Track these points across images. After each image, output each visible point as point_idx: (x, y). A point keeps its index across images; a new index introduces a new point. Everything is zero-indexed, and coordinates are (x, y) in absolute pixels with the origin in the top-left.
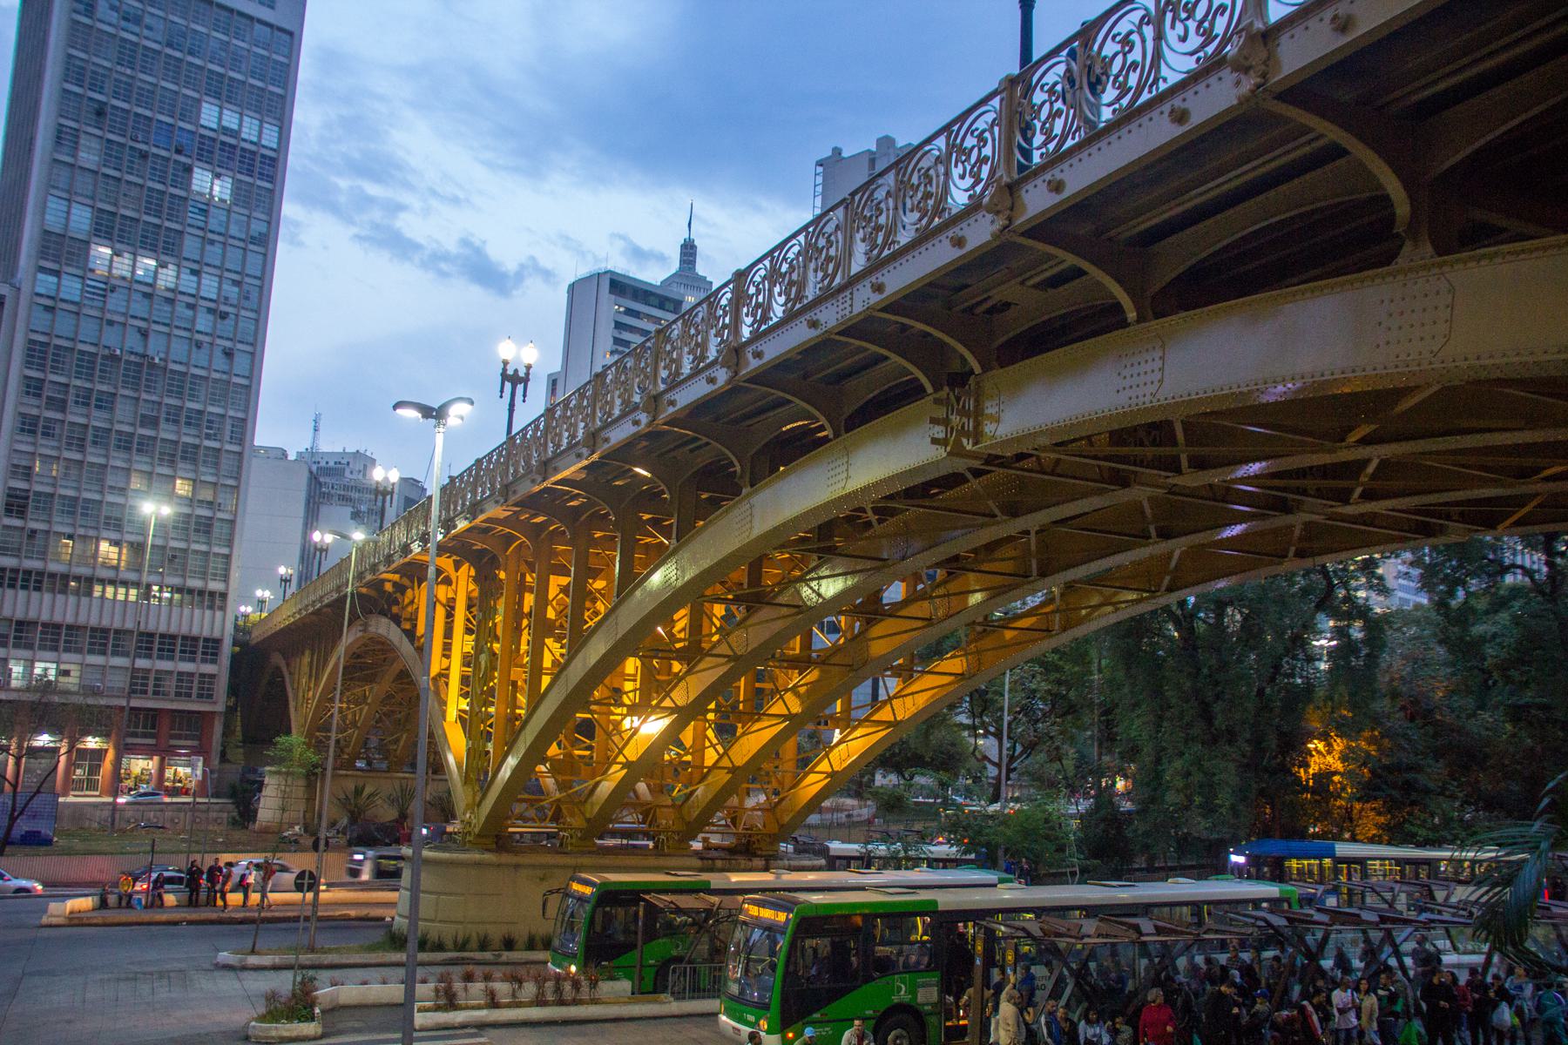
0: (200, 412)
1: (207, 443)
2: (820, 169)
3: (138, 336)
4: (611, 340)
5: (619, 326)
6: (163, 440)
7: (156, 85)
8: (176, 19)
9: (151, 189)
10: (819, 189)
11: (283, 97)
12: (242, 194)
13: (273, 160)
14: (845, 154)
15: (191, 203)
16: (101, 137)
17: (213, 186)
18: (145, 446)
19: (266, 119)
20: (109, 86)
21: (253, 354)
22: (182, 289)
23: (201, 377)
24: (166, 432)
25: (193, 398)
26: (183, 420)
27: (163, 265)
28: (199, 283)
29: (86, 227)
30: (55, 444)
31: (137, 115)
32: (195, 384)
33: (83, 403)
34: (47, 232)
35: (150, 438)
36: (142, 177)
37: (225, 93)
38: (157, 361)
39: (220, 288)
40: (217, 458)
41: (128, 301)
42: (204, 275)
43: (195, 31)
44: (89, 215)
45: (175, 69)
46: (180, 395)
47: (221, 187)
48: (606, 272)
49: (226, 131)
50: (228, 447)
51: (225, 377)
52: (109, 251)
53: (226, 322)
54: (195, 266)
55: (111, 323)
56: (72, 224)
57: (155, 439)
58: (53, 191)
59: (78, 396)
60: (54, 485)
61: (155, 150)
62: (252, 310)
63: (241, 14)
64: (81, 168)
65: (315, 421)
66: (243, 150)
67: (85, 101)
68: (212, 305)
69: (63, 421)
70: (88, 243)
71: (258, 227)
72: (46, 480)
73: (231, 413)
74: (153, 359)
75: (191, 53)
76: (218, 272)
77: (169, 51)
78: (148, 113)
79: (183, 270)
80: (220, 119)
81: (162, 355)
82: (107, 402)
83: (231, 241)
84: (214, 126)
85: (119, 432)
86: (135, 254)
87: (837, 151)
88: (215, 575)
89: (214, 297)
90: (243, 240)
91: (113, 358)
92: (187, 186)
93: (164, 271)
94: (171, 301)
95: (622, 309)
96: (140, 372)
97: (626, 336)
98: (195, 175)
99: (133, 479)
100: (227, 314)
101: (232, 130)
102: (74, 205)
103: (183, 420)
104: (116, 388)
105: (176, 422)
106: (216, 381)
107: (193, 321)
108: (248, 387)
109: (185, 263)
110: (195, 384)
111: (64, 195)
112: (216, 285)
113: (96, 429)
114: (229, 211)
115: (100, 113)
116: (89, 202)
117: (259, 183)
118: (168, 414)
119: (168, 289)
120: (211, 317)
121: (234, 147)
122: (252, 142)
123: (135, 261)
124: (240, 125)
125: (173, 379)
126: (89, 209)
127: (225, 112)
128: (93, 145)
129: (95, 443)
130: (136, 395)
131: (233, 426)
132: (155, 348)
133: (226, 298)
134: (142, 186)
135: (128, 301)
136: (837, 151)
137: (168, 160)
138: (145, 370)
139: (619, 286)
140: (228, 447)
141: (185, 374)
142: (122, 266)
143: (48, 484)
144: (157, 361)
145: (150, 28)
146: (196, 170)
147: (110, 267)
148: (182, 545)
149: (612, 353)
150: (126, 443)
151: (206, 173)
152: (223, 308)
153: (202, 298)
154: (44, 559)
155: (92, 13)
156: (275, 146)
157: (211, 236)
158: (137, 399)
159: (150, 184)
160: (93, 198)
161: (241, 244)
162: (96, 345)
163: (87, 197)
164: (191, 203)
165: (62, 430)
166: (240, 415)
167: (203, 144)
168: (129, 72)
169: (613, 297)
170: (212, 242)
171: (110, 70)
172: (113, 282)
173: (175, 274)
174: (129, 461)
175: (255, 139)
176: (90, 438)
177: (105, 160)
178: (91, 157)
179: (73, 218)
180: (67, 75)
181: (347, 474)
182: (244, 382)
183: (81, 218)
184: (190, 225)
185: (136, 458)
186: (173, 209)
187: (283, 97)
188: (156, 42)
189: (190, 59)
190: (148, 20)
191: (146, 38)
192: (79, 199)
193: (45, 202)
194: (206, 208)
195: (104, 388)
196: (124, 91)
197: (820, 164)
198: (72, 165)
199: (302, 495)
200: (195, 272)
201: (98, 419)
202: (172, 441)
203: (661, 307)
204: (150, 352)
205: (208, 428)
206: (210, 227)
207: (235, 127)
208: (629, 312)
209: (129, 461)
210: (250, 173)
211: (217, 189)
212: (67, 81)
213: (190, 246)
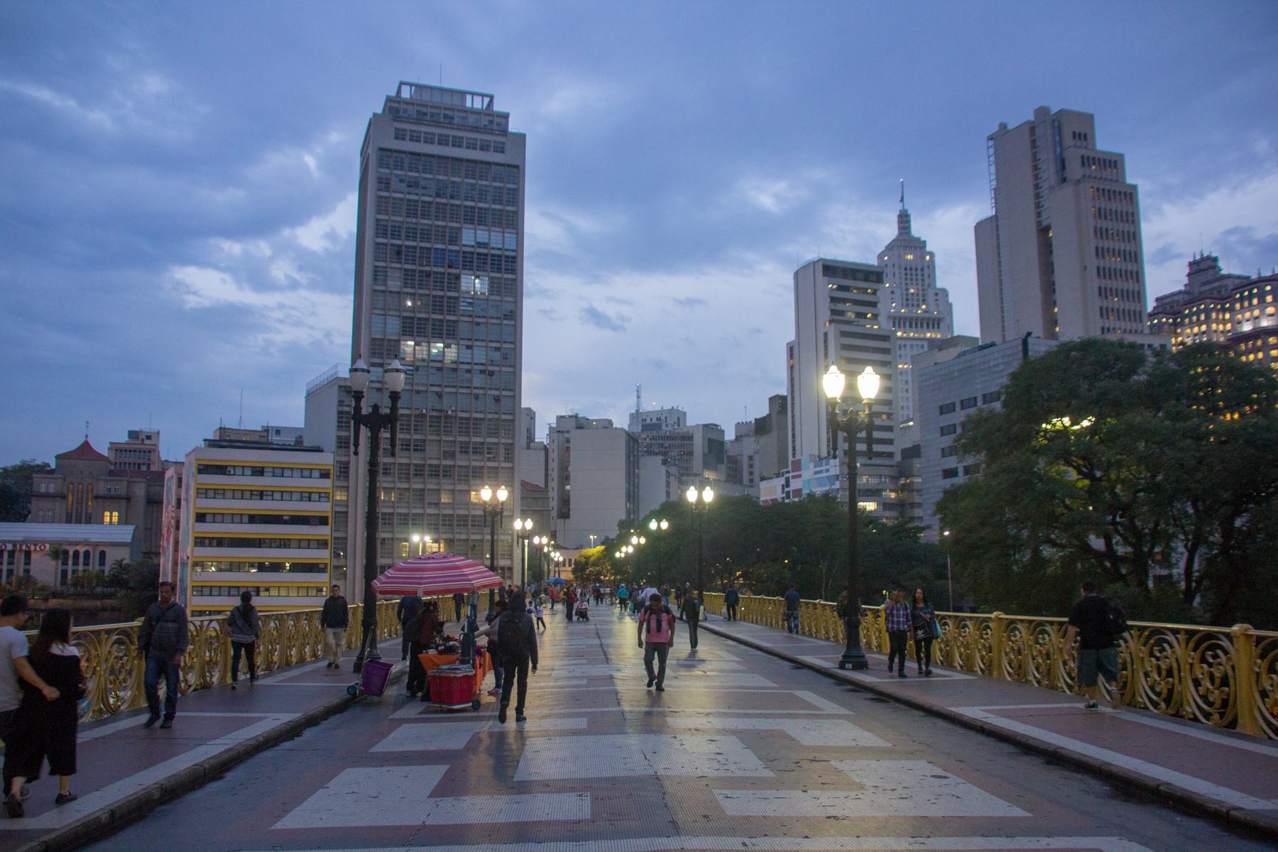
0: (482, 443)
1: (489, 464)
2: (991, 143)
3: (437, 397)
4: (829, 313)
5: (833, 300)
6: (460, 467)
7: (431, 225)
8: (440, 177)
9: (434, 296)
10: (992, 159)
11: (516, 213)
12: (494, 287)
13: (514, 258)
14: (1010, 127)
15: (462, 300)
16: (400, 269)
17: (475, 284)
18: (448, 472)
19: (506, 230)
20: (403, 234)
21: (514, 397)
22: (461, 360)
23: (481, 419)
24: (461, 461)
25: (477, 434)
26: (471, 450)
27: (447, 346)
28: (472, 354)
29: (397, 331)
30: (390, 479)
31: (421, 248)
32: (477, 424)
33: (406, 449)
34: (374, 339)
35: (451, 466)
36: (429, 289)
37: (476, 219)
38: (450, 412)
39: (487, 354)
40: (497, 473)
41: (427, 376)
42: (475, 348)
43: (454, 182)
44: (398, 322)
45: (442, 211)
46: (467, 434)
47: (481, 284)
48: (819, 261)
49: (480, 245)
50: (503, 465)
51: (496, 416)
52: (412, 343)
53: (494, 377)
54: (469, 343)
55: (418, 392)
56: (388, 330)
57: (454, 466)
58: (376, 311)
59: (402, 445)
60: (393, 507)
61: (435, 269)
62: (510, 366)
63: (482, 162)
64: (391, 292)
65: (637, 391)
66: (493, 255)
67: (389, 247)
68: (480, 367)
69: (394, 464)
70: (398, 341)
71: (507, 307)
72: (388, 504)
73: (503, 441)
74: (447, 412)
75: (452, 197)
76: (484, 344)
77: (438, 200)
78: (428, 245)
79: (460, 347)
80: (476, 237)
81: (453, 408)
82: (420, 447)
83: (491, 321)
84: (473, 243)
85: (430, 466)
86: (429, 343)
87: (1003, 126)
88: (504, 555)
89: (484, 362)
90: (499, 318)
91: (422, 416)
92: (457, 289)
93: (449, 350)
94: (455, 370)
95: (835, 287)
96: (439, 422)
97: (840, 307)
98: (462, 280)
99: (442, 496)
101: (484, 244)
102: (388, 317)
103: (471, 450)
104: (426, 436)
105: (467, 452)
106: (490, 420)
107: (471, 381)
108: (513, 421)
109: (462, 342)
110: (477, 424)
111: (382, 312)
112: (485, 353)
113: (416, 465)
114: (487, 300)
115: (399, 253)
116: (397, 313)
117: (506, 276)
118: (461, 448)
119: (453, 362)
120: (483, 376)
121: (486, 255)
122: (498, 249)
123: (429, 347)
124: (489, 239)
125: (462, 423)
126: (398, 318)
127: (478, 232)
128: (396, 275)
129: (416, 475)
130: (438, 438)
131: (505, 450)
132: (446, 403)
133: (492, 361)
134: (429, 295)
135: (427, 376)
136: (1003, 126)
137: (443, 274)
138: (443, 420)
139: (831, 269)
140: (503, 465)
141: (468, 419)
142: (422, 352)
143: (390, 507)
144: (450, 412)
145: (424, 188)
146: (463, 276)
147: (414, 354)
149: (831, 322)
150: (435, 472)
151: (469, 277)
152: (491, 368)
153: (476, 364)
154: (392, 558)
155: (389, 187)
156: (515, 248)
157: (477, 320)
158: (440, 441)
159: (434, 293)
160: (399, 310)
161: (498, 321)
162: (410, 409)
163: (395, 310)
164: (462, 300)
165: (394, 469)
166: (509, 441)
167: (466, 257)
168: (414, 220)
169: (826, 278)
170: (478, 324)
171: (402, 222)
172: (417, 364)
174: (439, 484)
175: (500, 246)
176: (412, 472)
177: (405, 283)
178: (396, 283)
179: (388, 326)
180: (377, 233)
181: (664, 427)
182: (510, 417)
183: (394, 325)
184: (462, 315)
185: (442, 481)
186: (450, 307)
187: (516, 213)
188: (429, 196)
189: (453, 202)
190: (422, 183)
191: (423, 195)
192: (392, 313)
193: (371, 322)
194: (474, 300)
195: (418, 437)
196: (412, 234)
197: (990, 138)
198: (383, 292)
199: (623, 452)
200: (469, 347)
201: (416, 459)
202: (465, 466)
203: (866, 279)
204: (445, 408)
205: (488, 453)
206: (475, 314)
207: (487, 241)
208: (841, 288)
209: (439, 484)
210: (499, 270)
211: (478, 286)
212: (377, 237)
213: (463, 329)
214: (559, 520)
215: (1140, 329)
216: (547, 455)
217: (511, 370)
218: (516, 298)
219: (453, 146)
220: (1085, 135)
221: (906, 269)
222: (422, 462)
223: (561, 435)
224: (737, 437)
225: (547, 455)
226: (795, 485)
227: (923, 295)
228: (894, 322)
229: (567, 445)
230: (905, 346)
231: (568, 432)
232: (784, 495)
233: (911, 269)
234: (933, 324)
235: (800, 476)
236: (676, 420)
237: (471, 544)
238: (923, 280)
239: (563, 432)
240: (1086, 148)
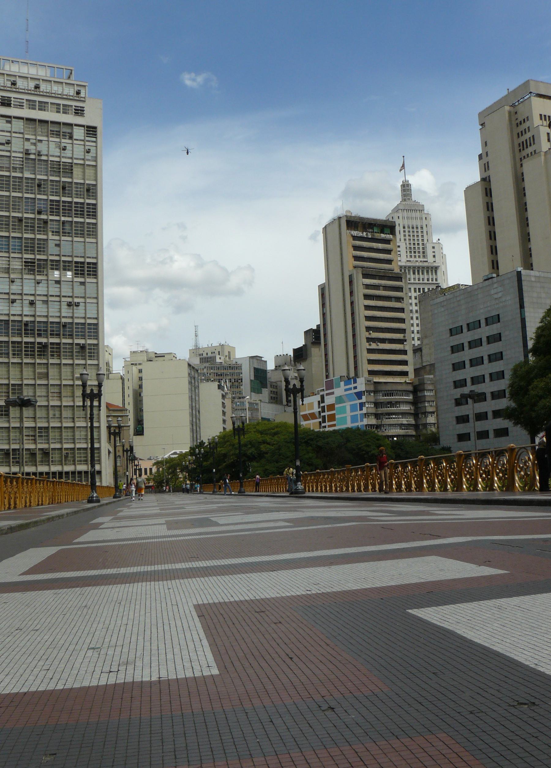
53: (80, 307)
61: (26, 215)
100: (78, 303)
148: (72, 446)
152: (76, 300)
158: (34, 364)
173: (46, 285)
186: (40, 248)
214: (135, 437)
216: (123, 384)
217: (95, 301)
218: (96, 238)
219: (39, 109)
222: (20, 383)
223: (134, 368)
224: (276, 367)
225: (123, 384)
226: (329, 400)
229: (140, 375)
231: (140, 364)
232: (320, 410)
235: (333, 393)
236: (227, 354)
237: (64, 452)
239: (136, 364)
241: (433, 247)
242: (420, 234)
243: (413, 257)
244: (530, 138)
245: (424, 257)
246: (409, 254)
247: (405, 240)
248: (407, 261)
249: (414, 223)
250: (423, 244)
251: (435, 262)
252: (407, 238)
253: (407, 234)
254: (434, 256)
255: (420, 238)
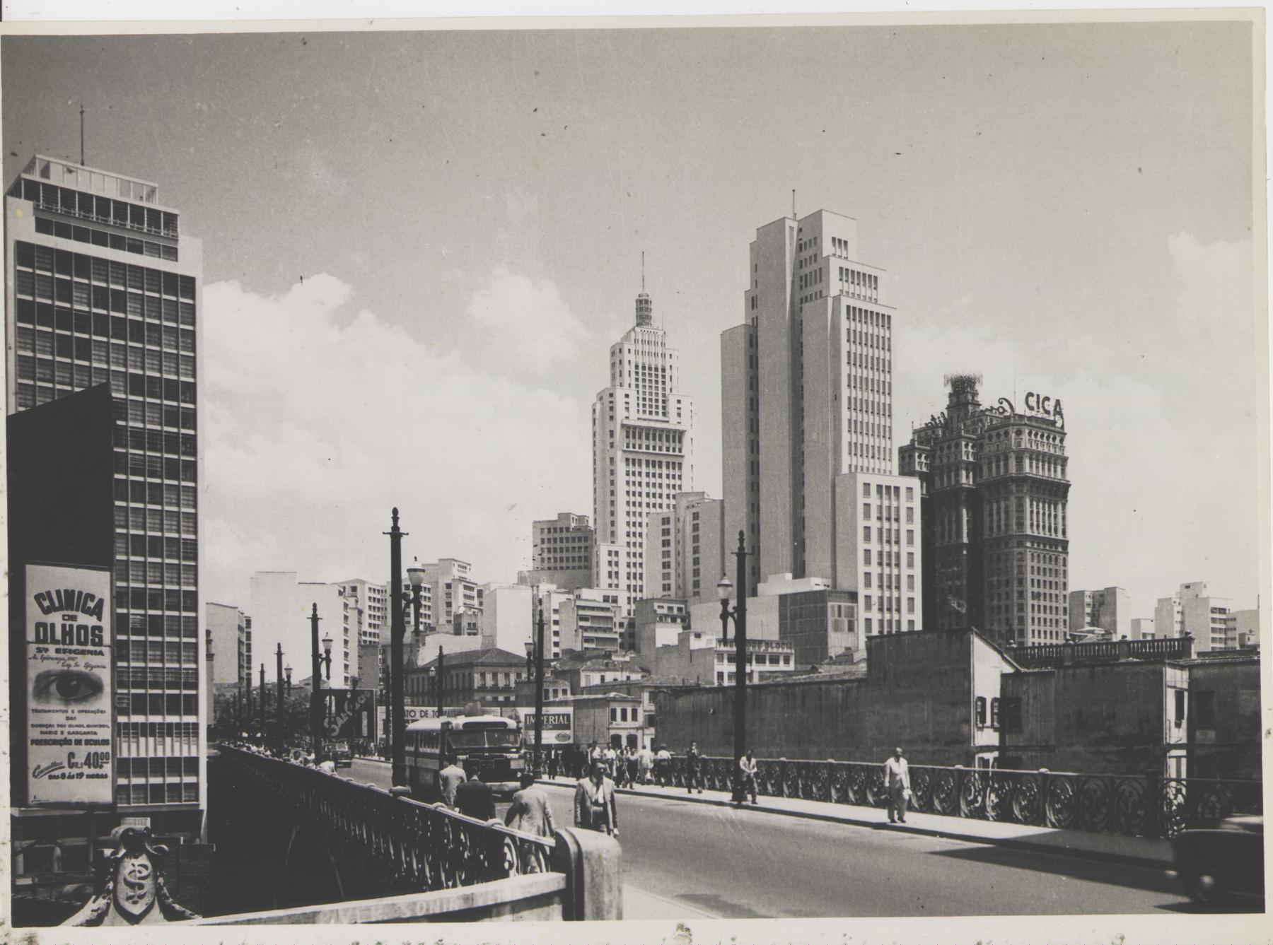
215: (888, 469)
220: (846, 242)
221: (644, 368)
227: (664, 402)
228: (628, 432)
230: (640, 461)
233: (650, 368)
234: (674, 437)
238: (664, 383)
240: (846, 258)
241: (679, 402)
242: (660, 379)
243: (654, 413)
244: (816, 271)
245: (664, 414)
246: (641, 408)
247: (637, 386)
248: (639, 419)
249: (653, 361)
250: (664, 395)
251: (679, 423)
252: (640, 383)
253: (640, 377)
254: (679, 415)
255: (660, 385)
